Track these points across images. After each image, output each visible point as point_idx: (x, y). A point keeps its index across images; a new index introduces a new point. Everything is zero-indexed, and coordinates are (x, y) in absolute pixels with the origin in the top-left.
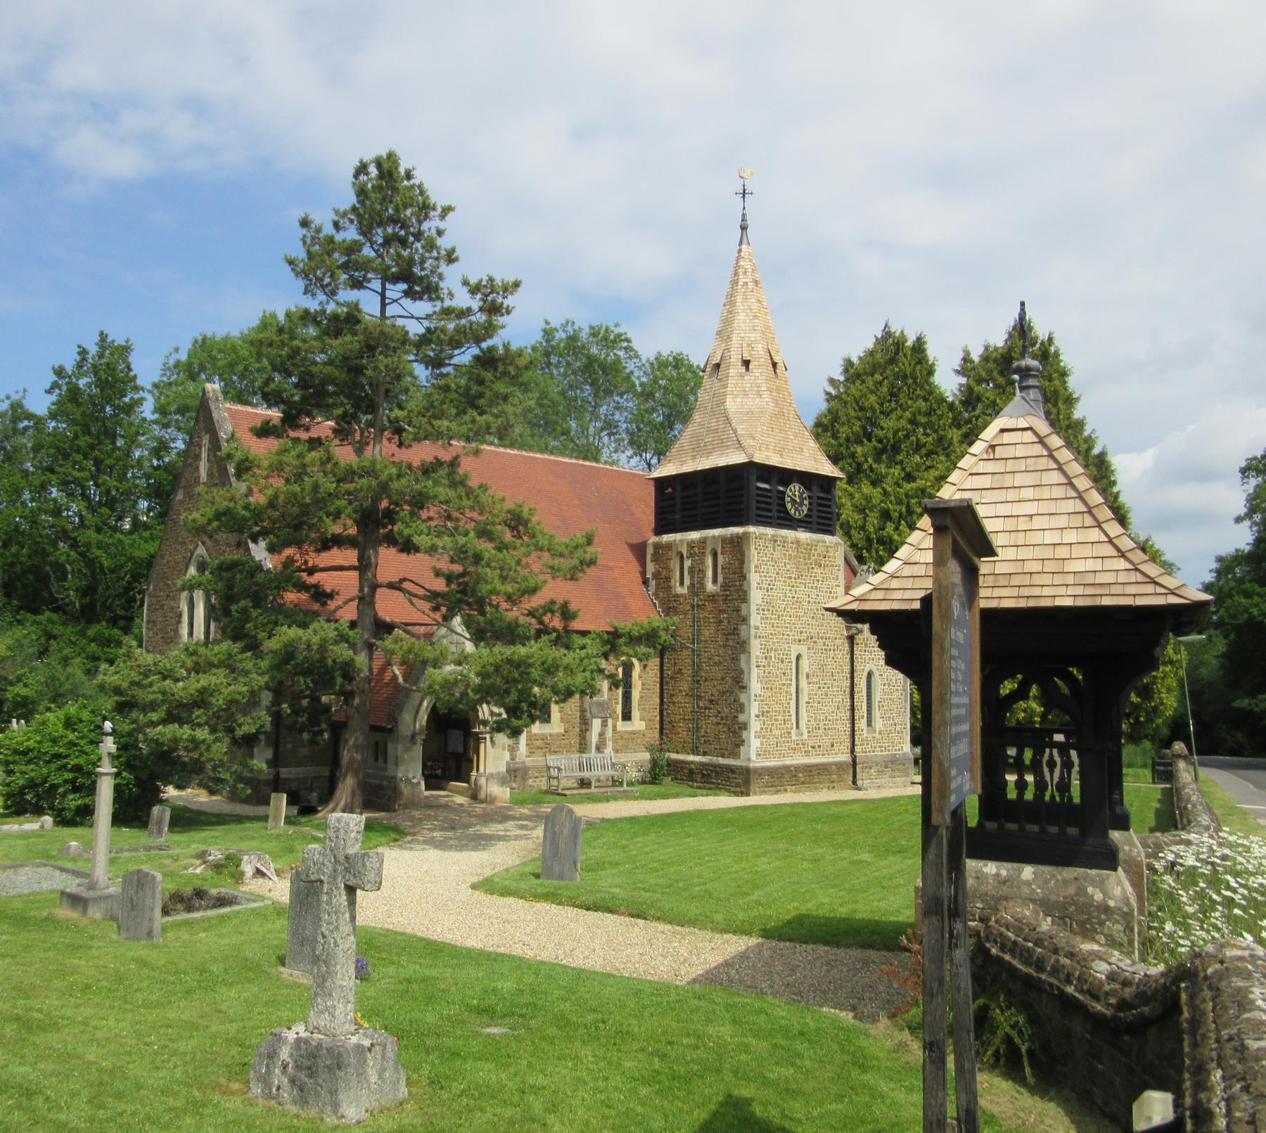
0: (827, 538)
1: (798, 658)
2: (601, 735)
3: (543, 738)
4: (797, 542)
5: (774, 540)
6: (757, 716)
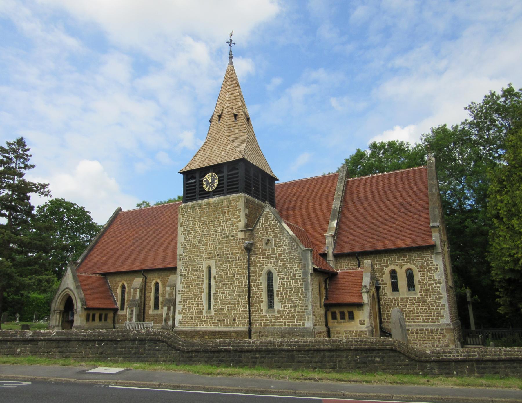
0: (231, 196)
1: (209, 269)
2: (168, 314)
3: (154, 316)
4: (209, 204)
5: (193, 207)
6: (180, 302)
